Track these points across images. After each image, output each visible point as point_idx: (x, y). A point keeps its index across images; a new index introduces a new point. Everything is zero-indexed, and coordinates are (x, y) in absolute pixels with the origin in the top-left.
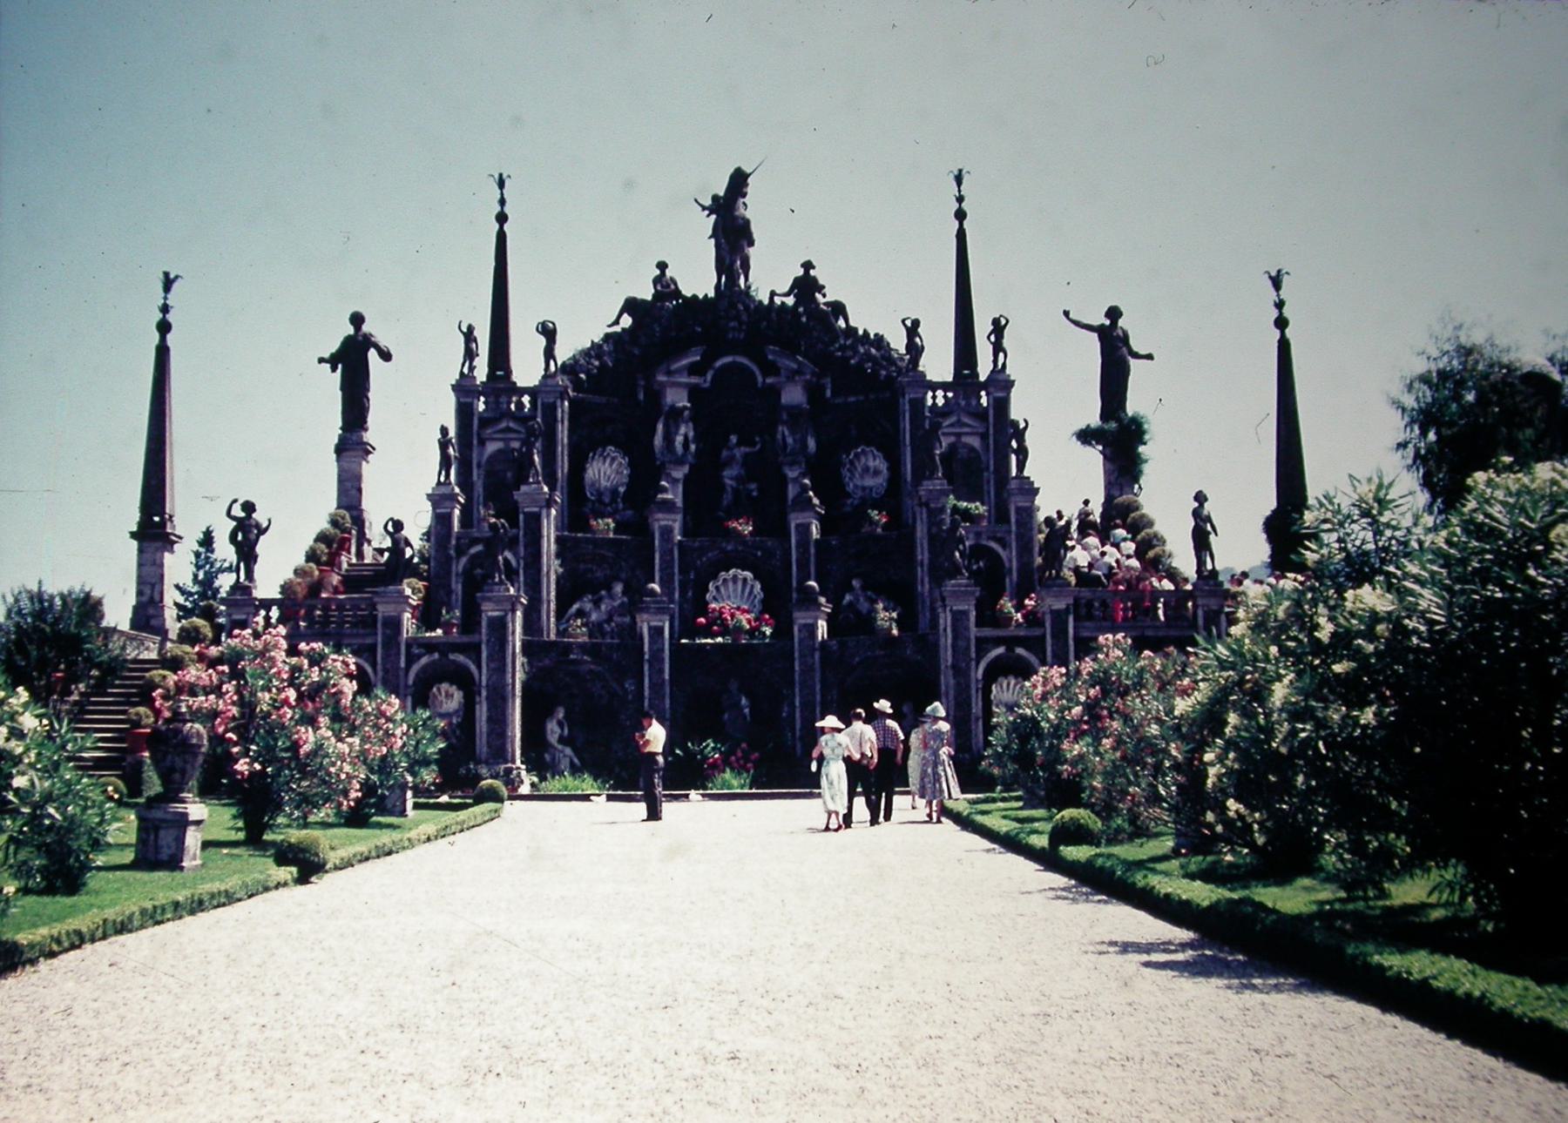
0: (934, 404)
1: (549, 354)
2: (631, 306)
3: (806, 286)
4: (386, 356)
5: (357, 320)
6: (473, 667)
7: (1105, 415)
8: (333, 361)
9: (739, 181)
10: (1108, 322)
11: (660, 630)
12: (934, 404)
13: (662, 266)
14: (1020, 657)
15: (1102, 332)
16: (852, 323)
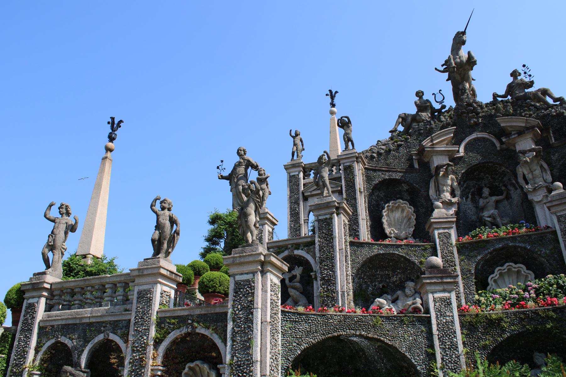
1: (348, 139)
2: (404, 119)
8: (229, 178)
9: (459, 40)
11: (447, 303)
13: (419, 94)
16: (557, 96)
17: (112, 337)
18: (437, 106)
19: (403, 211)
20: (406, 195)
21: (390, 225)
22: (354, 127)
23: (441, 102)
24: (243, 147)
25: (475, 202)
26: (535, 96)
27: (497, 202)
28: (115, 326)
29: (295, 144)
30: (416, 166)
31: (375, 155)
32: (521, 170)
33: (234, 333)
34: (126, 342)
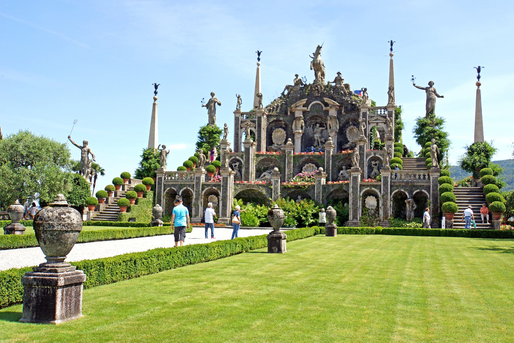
0: (381, 114)
2: (287, 87)
3: (338, 80)
4: (219, 104)
5: (212, 95)
6: (219, 192)
7: (428, 114)
8: (208, 106)
10: (429, 86)
11: (277, 181)
12: (381, 114)
13: (297, 76)
14: (373, 190)
15: (427, 89)
17: (188, 188)
18: (304, 83)
19: (281, 132)
20: (284, 126)
21: (275, 138)
22: (263, 98)
23: (305, 82)
24: (214, 92)
25: (313, 128)
26: (342, 89)
27: (322, 130)
28: (189, 186)
29: (238, 102)
30: (289, 114)
31: (272, 109)
32: (329, 122)
33: (223, 189)
34: (193, 190)
